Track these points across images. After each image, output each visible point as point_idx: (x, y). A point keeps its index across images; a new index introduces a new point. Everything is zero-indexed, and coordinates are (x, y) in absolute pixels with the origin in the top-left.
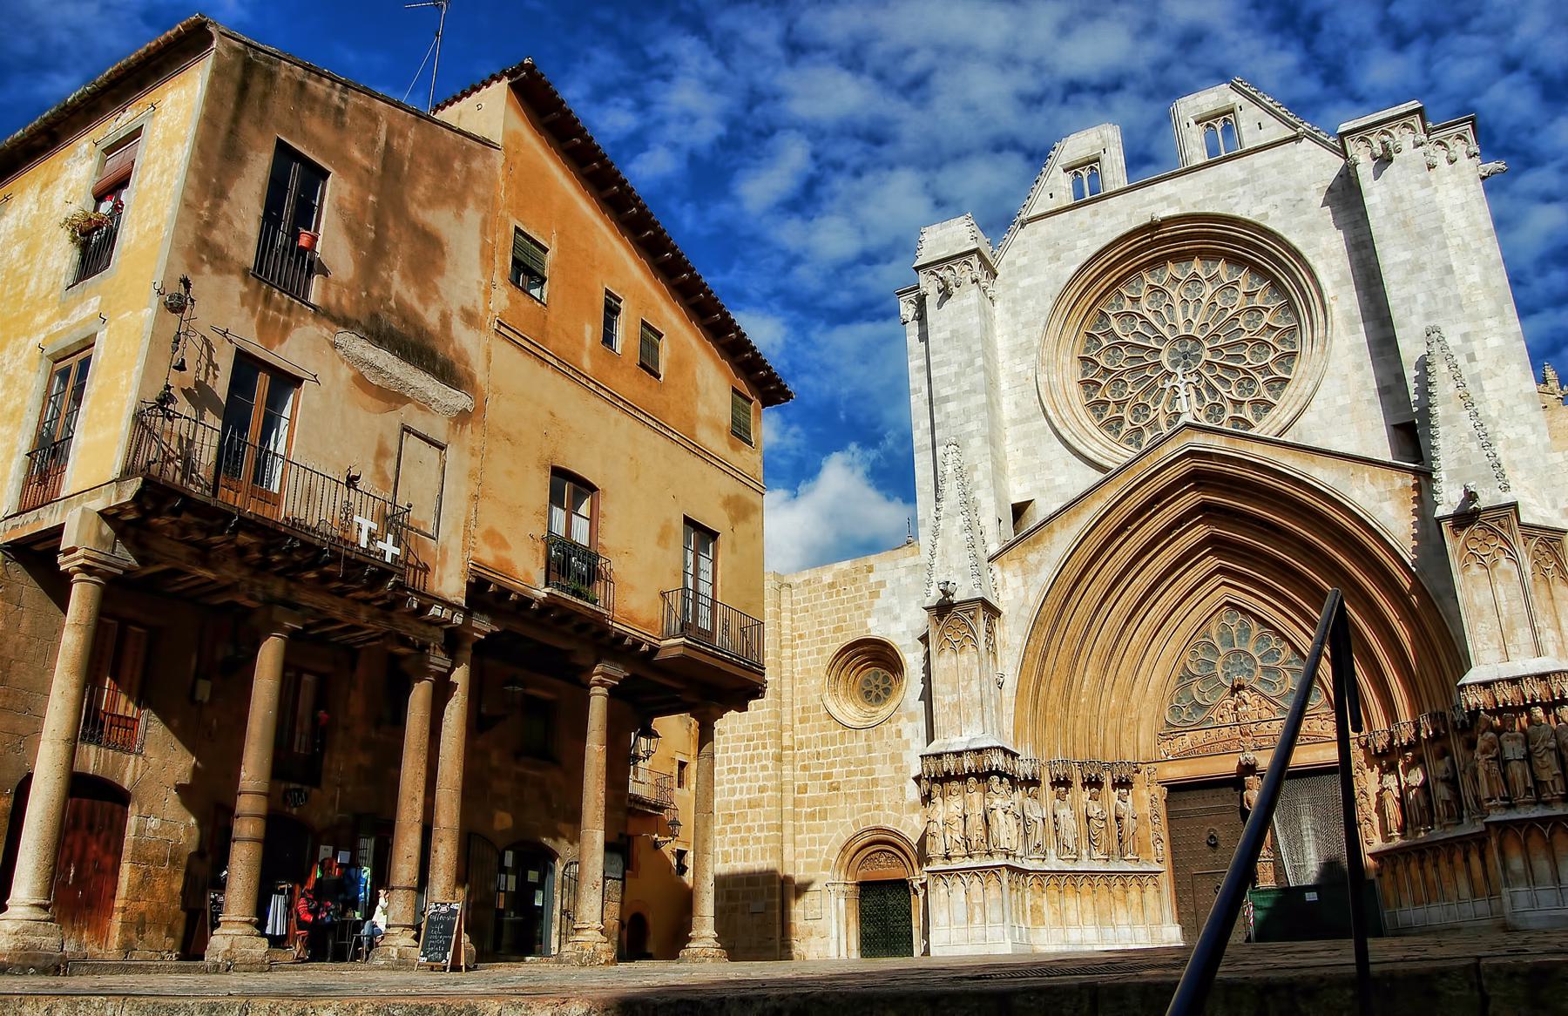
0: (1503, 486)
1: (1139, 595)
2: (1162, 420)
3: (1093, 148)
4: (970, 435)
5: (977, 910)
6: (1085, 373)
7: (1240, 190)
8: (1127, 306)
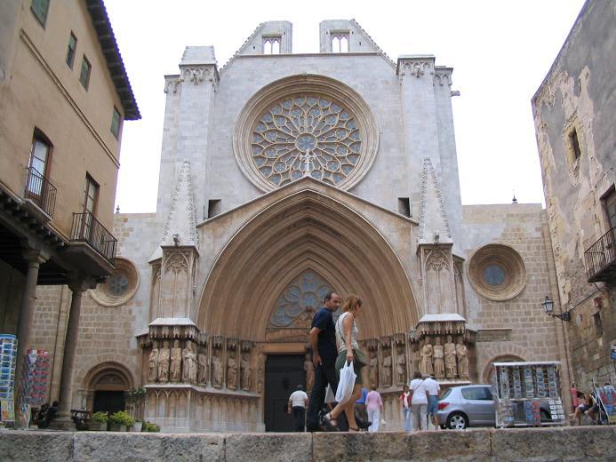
2: (290, 172)
4: (196, 160)
5: (172, 410)
6: (255, 141)
7: (346, 71)
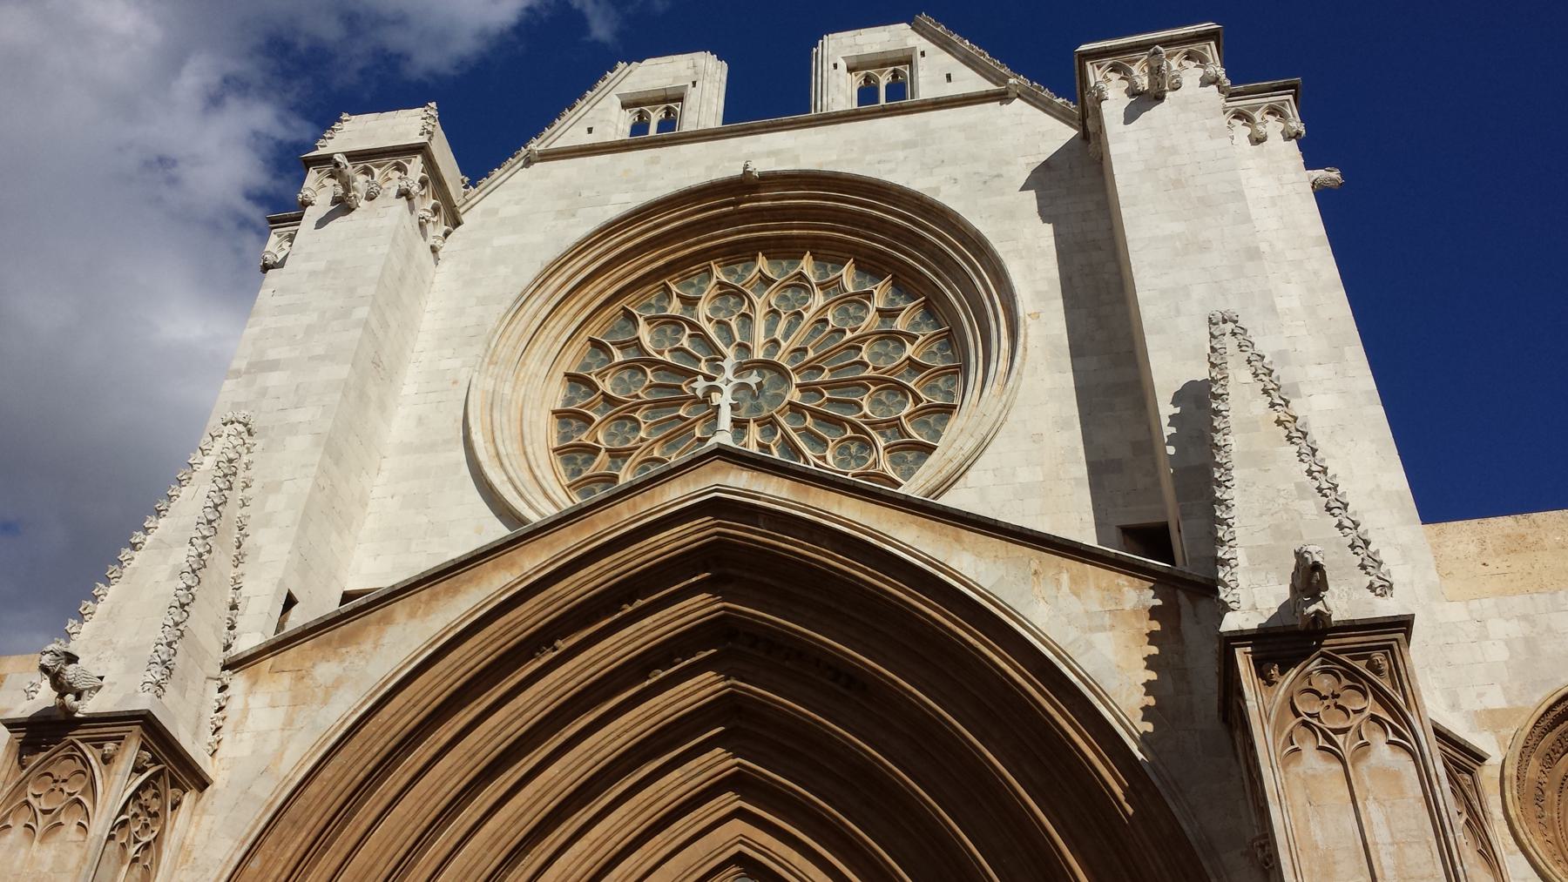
0: (1378, 583)
1: (549, 804)
3: (676, 78)
7: (901, 155)
8: (675, 308)
